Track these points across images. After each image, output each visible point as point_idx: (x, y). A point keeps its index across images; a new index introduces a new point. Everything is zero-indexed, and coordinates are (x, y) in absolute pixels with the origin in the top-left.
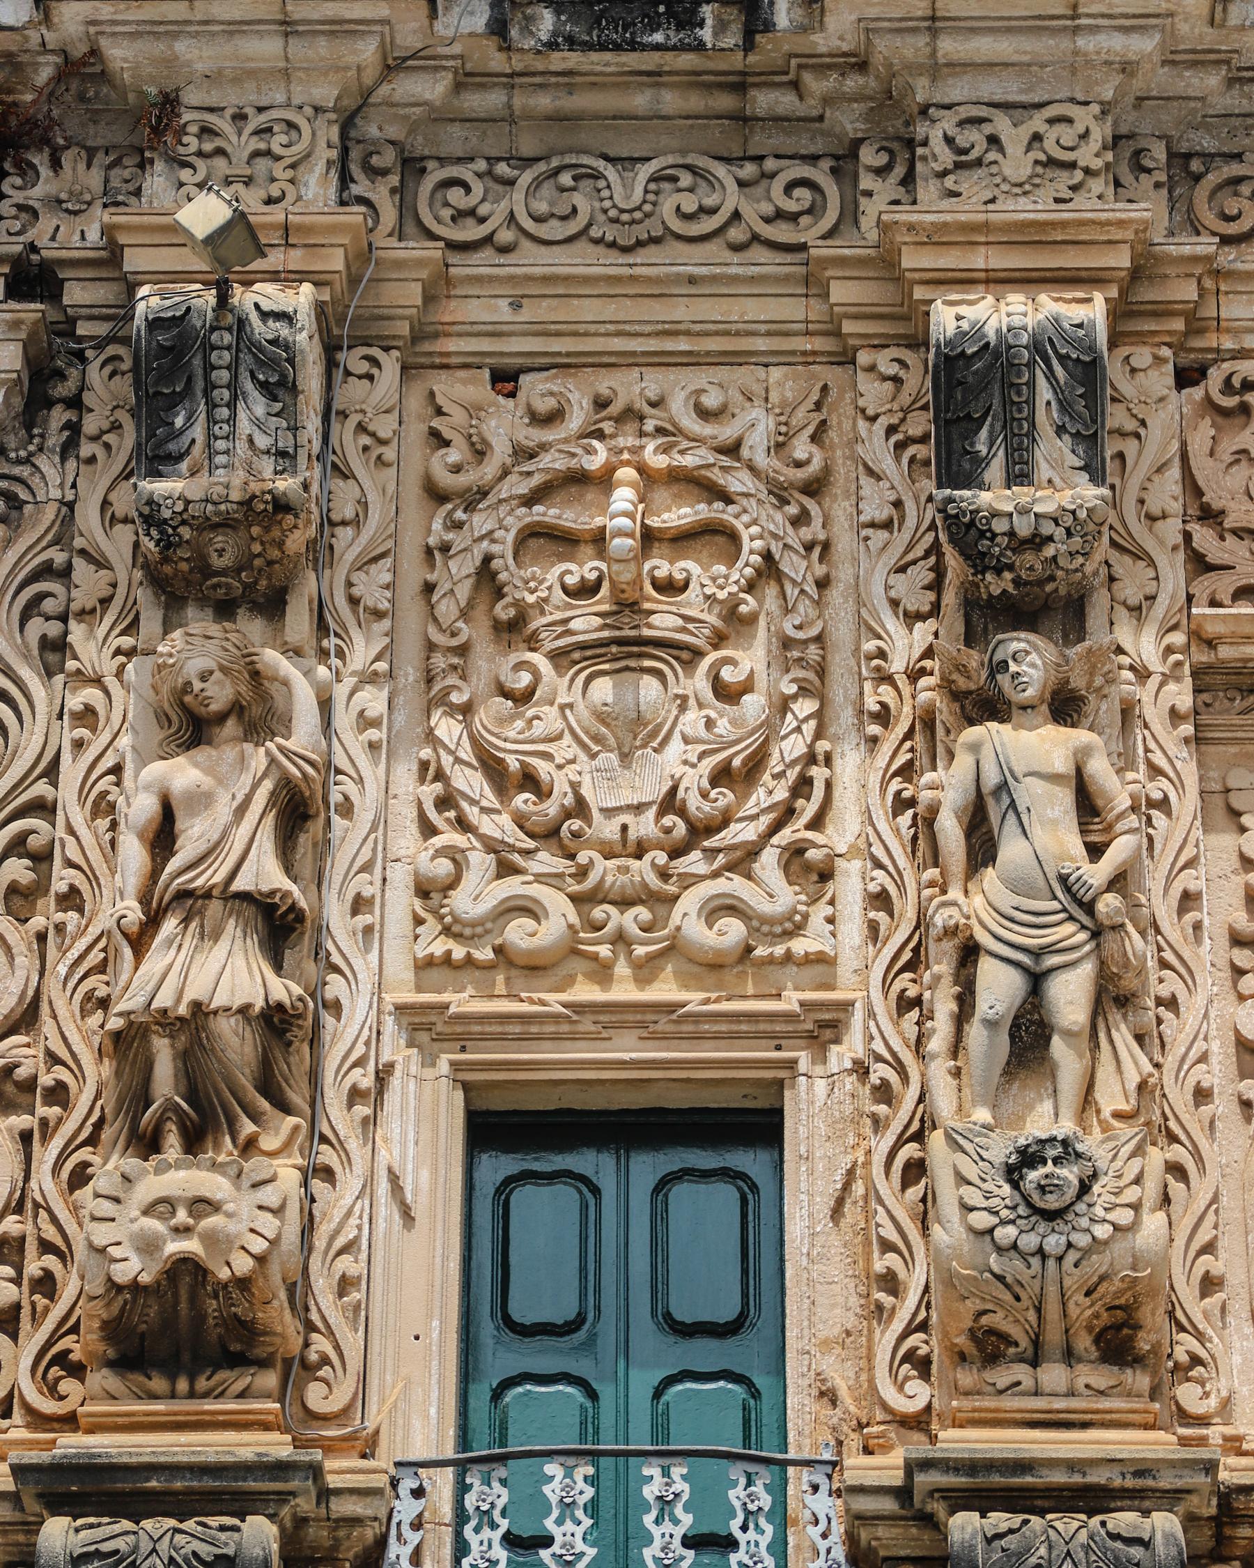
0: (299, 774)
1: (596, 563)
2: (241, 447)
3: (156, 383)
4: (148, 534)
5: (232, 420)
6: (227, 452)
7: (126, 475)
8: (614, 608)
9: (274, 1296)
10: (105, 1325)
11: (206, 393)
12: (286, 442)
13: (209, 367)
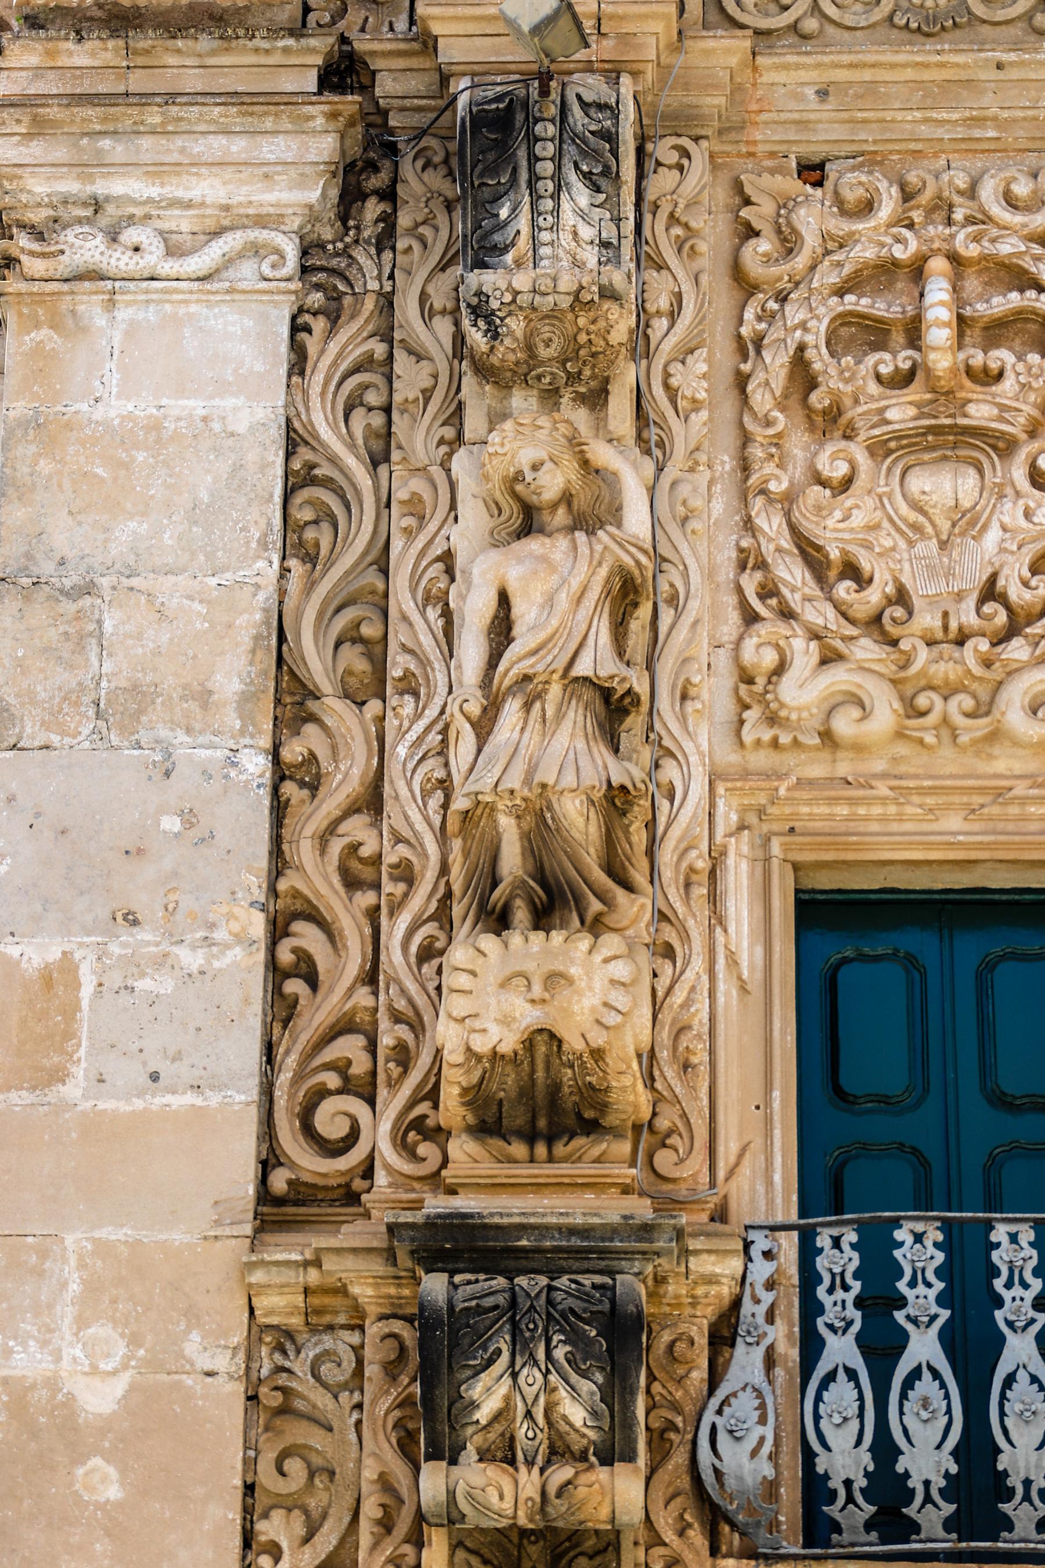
0: (632, 563)
1: (910, 352)
2: (565, 238)
3: (481, 175)
4: (475, 325)
5: (557, 210)
6: (552, 243)
7: (443, 267)
8: (928, 396)
9: (629, 1067)
10: (465, 1091)
11: (531, 185)
12: (609, 232)
13: (533, 159)
